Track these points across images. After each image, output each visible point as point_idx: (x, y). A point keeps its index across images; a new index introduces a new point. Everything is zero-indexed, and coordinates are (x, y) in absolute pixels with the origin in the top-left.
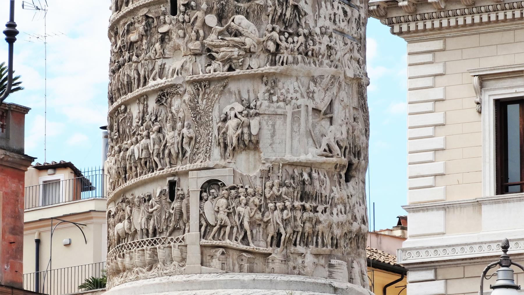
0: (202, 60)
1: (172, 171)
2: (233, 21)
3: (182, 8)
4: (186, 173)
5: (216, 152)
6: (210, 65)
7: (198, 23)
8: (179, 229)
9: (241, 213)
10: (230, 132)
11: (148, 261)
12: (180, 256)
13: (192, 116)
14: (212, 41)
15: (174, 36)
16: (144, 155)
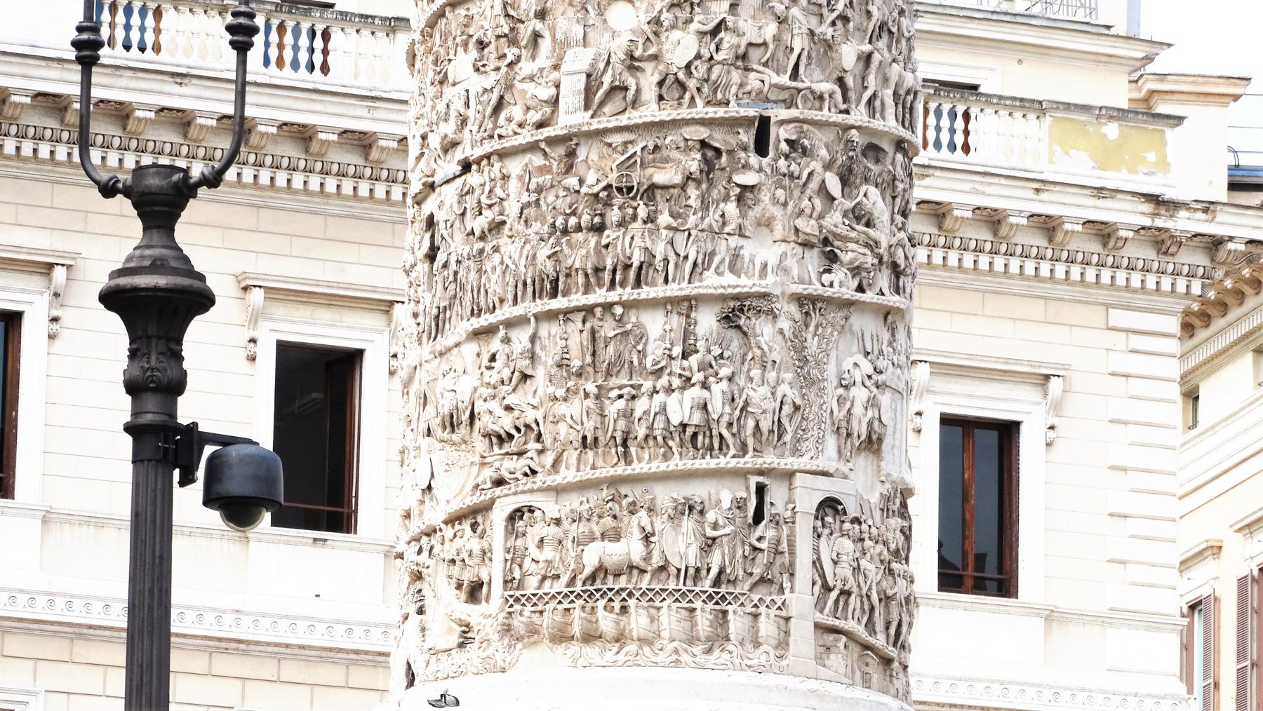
0: (813, 260)
1: (766, 466)
2: (865, 195)
3: (784, 147)
4: (789, 475)
5: (831, 443)
6: (829, 271)
7: (814, 185)
8: (770, 582)
9: (866, 572)
10: (858, 410)
11: (706, 634)
12: (777, 637)
13: (794, 365)
14: (836, 226)
15: (765, 196)
16: (697, 418)
